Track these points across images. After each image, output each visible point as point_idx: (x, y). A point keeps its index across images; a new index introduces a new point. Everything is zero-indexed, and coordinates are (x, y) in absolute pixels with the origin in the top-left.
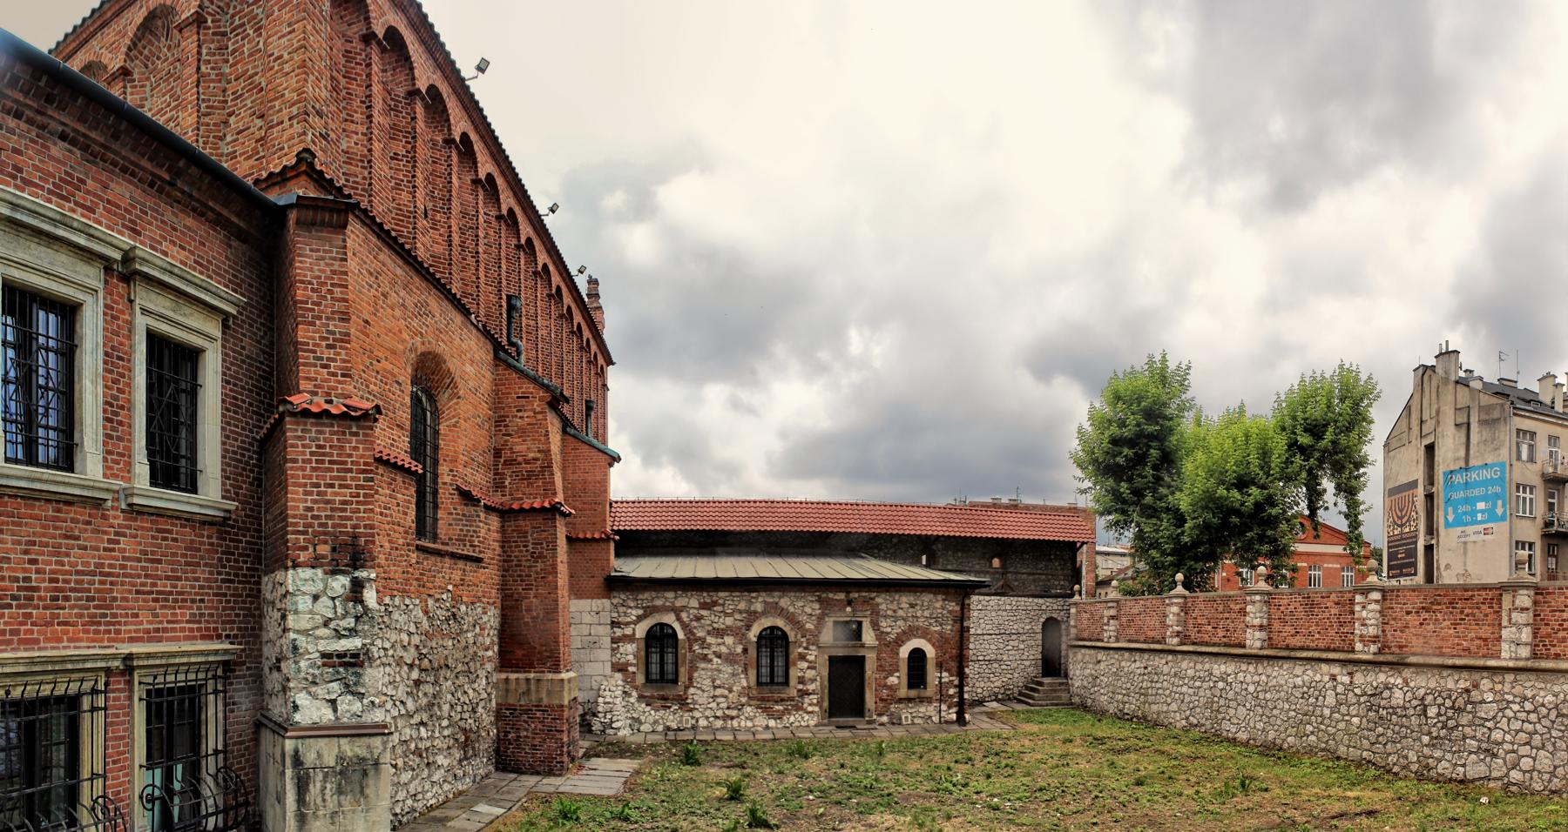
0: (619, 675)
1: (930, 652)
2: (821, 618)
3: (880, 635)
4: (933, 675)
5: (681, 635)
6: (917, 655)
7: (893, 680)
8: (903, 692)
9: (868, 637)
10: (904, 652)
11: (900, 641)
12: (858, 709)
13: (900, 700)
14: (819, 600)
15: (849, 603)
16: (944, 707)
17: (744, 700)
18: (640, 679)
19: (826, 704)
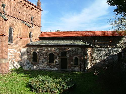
0: (28, 60)
1: (79, 58)
2: (59, 52)
3: (70, 55)
4: (79, 63)
5: (37, 54)
6: (76, 58)
7: (71, 63)
8: (73, 65)
9: (68, 55)
10: (74, 58)
11: (73, 56)
12: (66, 68)
13: (73, 67)
14: (59, 48)
15: (64, 49)
16: (81, 68)
17: (47, 65)
18: (31, 61)
19: (60, 66)
